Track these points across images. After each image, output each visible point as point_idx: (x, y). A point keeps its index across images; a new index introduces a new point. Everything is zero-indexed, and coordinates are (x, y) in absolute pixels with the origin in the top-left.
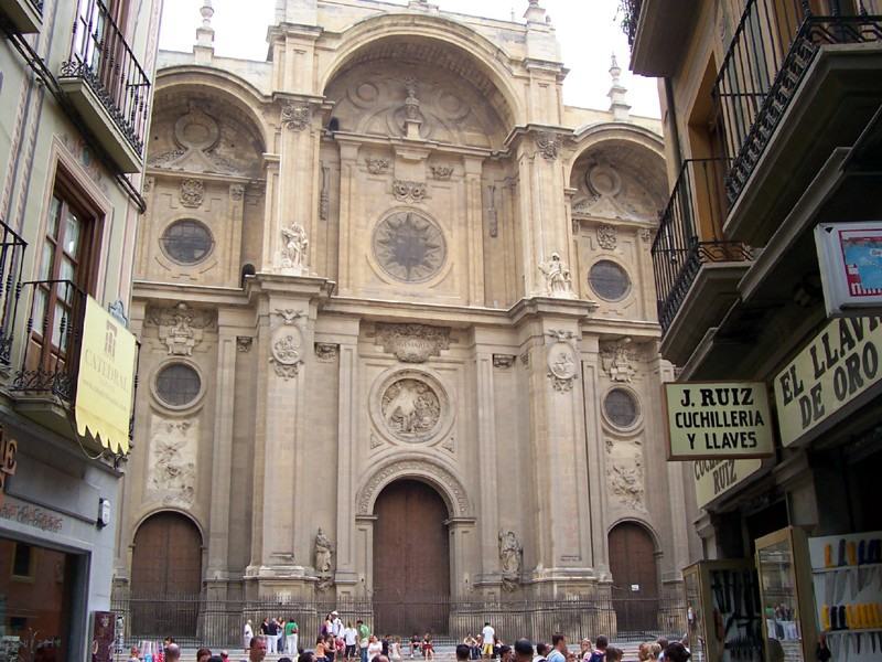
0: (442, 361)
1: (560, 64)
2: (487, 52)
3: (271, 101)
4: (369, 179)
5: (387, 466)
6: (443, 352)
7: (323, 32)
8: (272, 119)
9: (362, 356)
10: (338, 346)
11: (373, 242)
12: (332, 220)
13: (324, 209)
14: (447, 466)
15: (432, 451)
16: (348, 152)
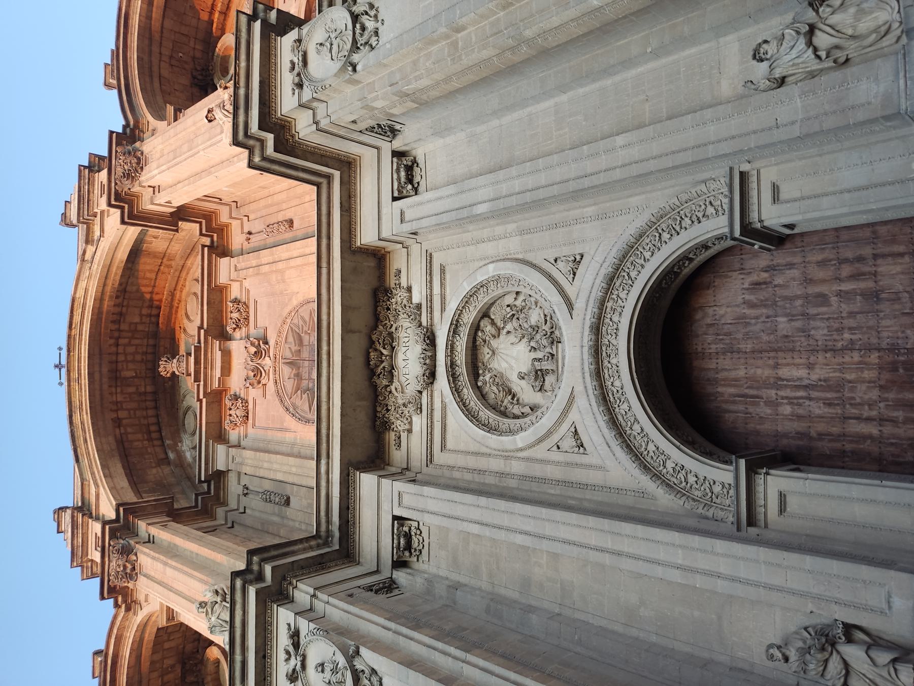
0: (430, 299)
1: (80, 171)
2: (89, 277)
3: (120, 599)
4: (254, 425)
5: (614, 422)
6: (416, 299)
7: (79, 509)
8: (141, 598)
9: (430, 459)
10: (395, 518)
11: (308, 421)
12: (288, 490)
13: (277, 500)
14: (607, 269)
15: (579, 305)
16: (221, 457)
